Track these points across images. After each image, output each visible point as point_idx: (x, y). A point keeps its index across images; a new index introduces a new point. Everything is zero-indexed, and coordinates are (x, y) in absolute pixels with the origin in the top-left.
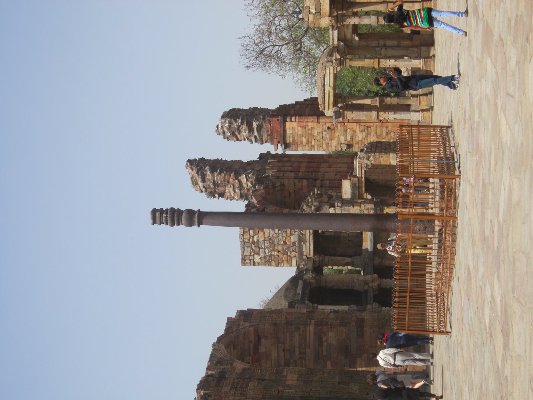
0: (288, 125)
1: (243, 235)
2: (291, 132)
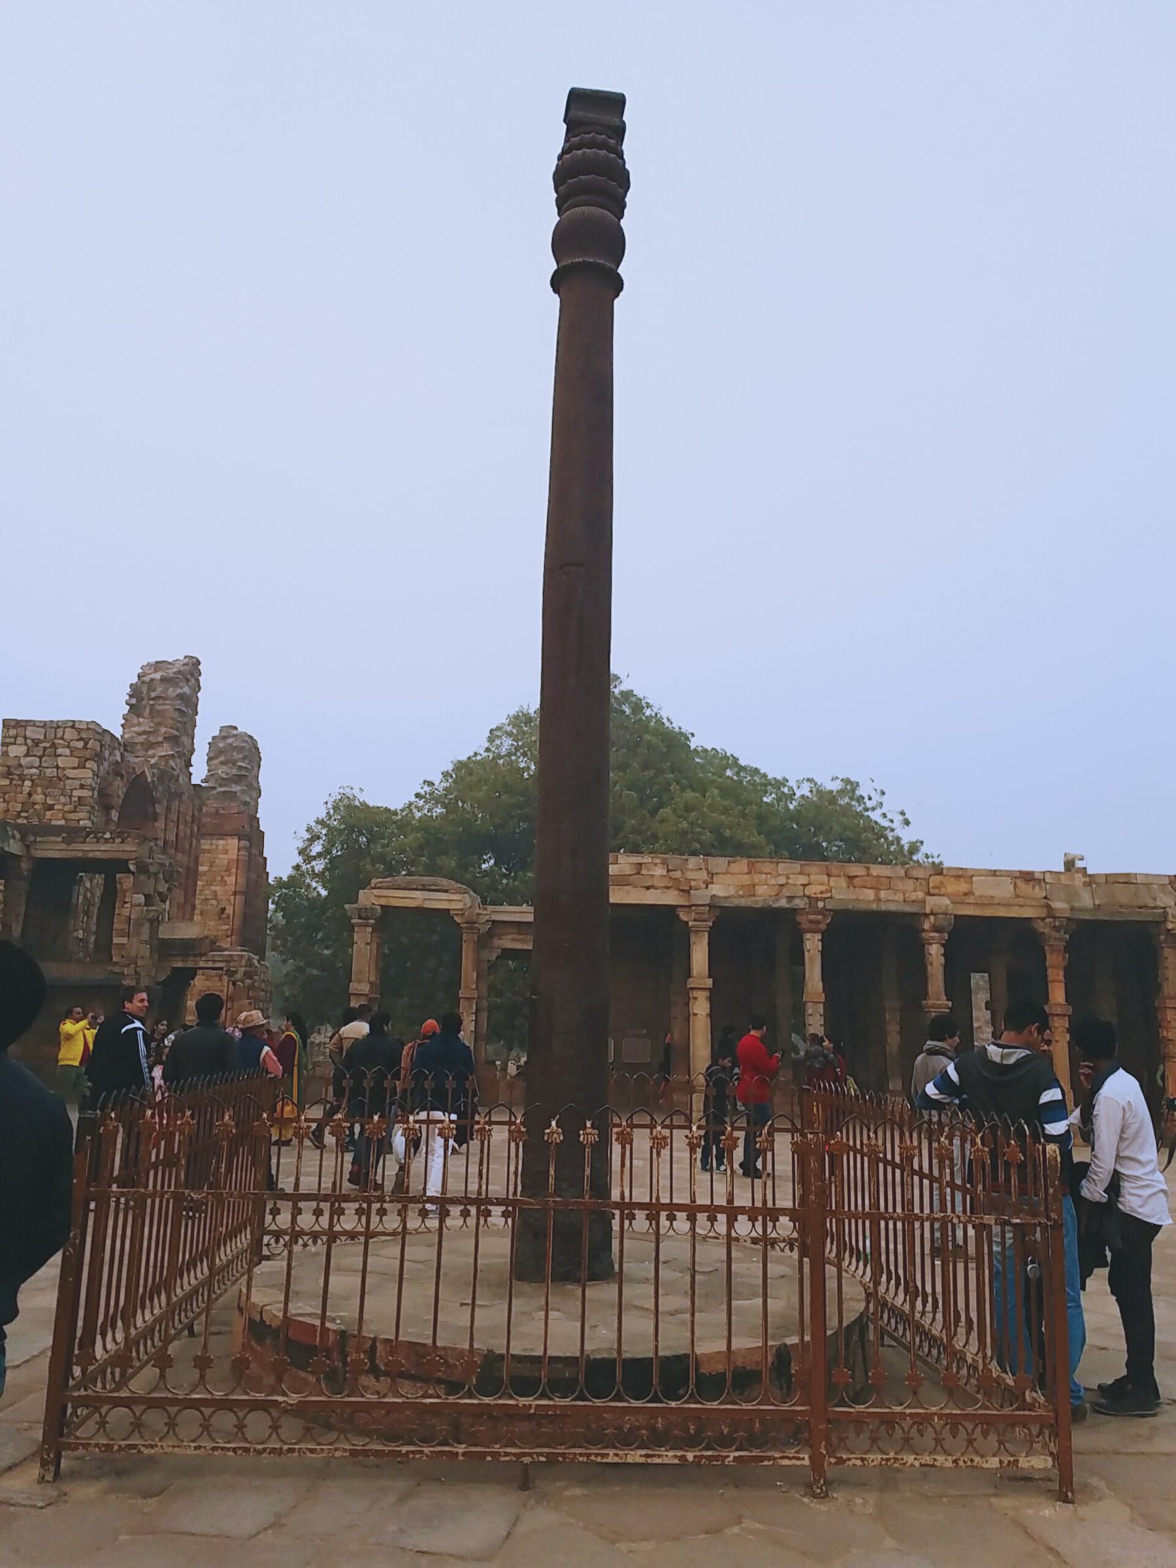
0: (233, 843)
1: (73, 727)
2: (220, 847)
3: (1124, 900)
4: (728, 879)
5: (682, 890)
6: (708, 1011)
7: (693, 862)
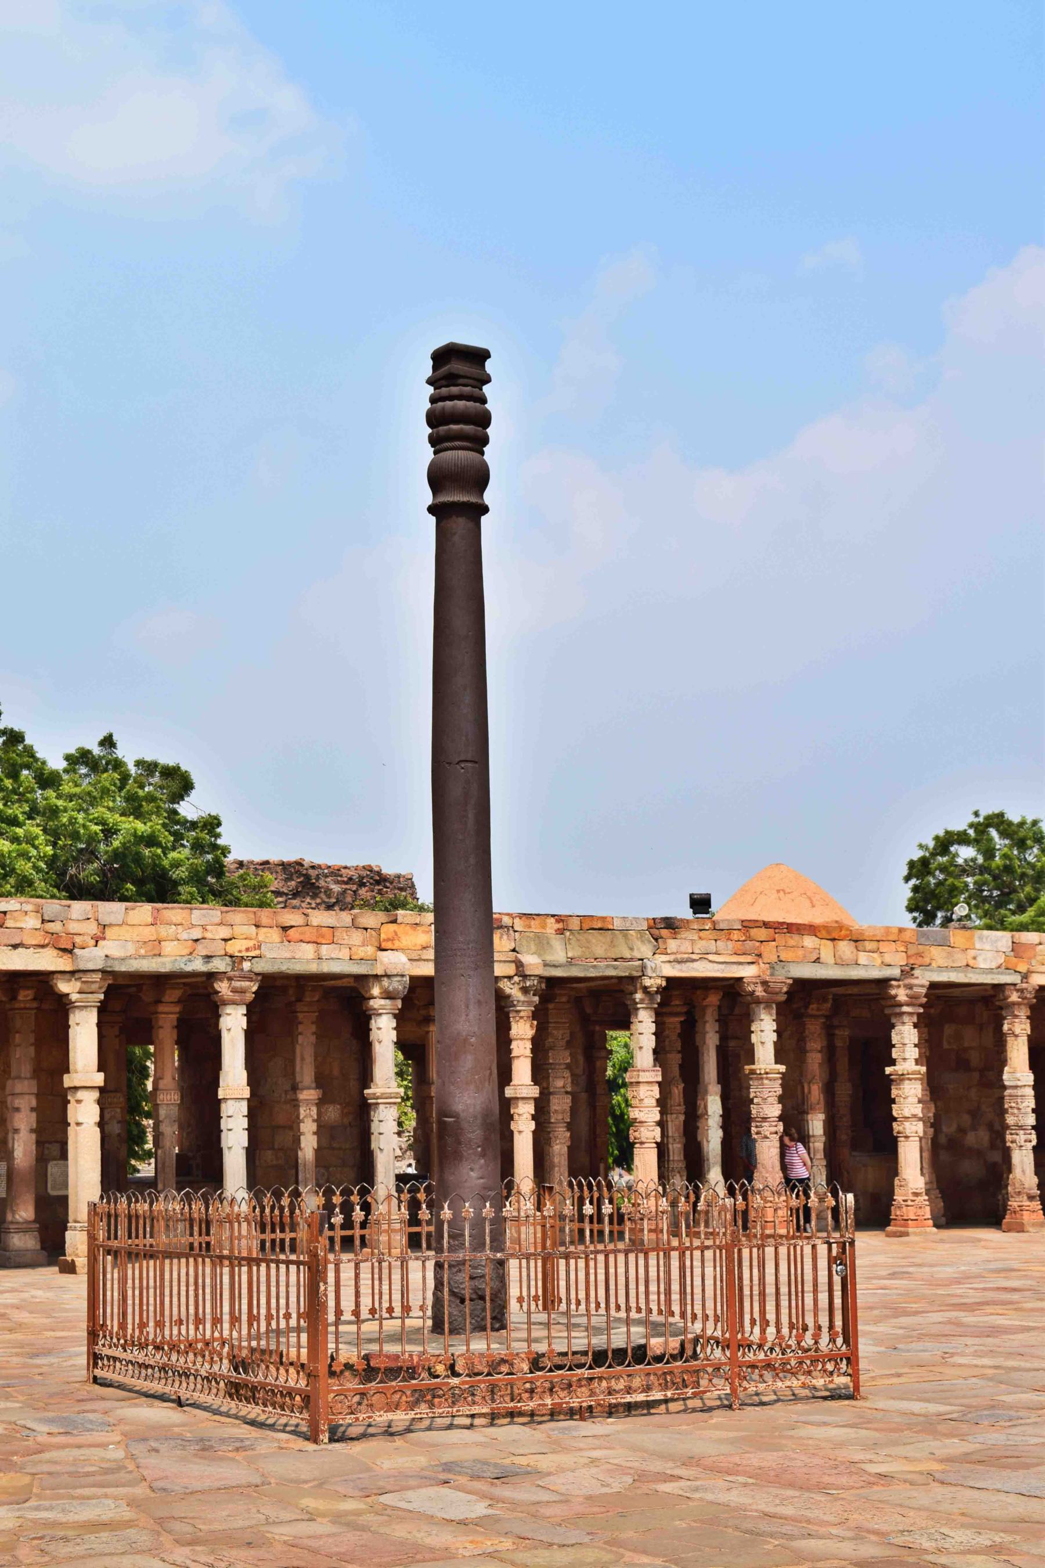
3: (600, 951)
4: (125, 932)
5: (64, 950)
6: (98, 1119)
7: (80, 908)
